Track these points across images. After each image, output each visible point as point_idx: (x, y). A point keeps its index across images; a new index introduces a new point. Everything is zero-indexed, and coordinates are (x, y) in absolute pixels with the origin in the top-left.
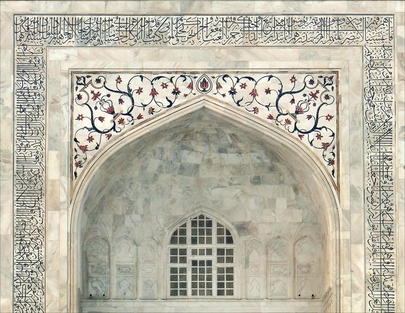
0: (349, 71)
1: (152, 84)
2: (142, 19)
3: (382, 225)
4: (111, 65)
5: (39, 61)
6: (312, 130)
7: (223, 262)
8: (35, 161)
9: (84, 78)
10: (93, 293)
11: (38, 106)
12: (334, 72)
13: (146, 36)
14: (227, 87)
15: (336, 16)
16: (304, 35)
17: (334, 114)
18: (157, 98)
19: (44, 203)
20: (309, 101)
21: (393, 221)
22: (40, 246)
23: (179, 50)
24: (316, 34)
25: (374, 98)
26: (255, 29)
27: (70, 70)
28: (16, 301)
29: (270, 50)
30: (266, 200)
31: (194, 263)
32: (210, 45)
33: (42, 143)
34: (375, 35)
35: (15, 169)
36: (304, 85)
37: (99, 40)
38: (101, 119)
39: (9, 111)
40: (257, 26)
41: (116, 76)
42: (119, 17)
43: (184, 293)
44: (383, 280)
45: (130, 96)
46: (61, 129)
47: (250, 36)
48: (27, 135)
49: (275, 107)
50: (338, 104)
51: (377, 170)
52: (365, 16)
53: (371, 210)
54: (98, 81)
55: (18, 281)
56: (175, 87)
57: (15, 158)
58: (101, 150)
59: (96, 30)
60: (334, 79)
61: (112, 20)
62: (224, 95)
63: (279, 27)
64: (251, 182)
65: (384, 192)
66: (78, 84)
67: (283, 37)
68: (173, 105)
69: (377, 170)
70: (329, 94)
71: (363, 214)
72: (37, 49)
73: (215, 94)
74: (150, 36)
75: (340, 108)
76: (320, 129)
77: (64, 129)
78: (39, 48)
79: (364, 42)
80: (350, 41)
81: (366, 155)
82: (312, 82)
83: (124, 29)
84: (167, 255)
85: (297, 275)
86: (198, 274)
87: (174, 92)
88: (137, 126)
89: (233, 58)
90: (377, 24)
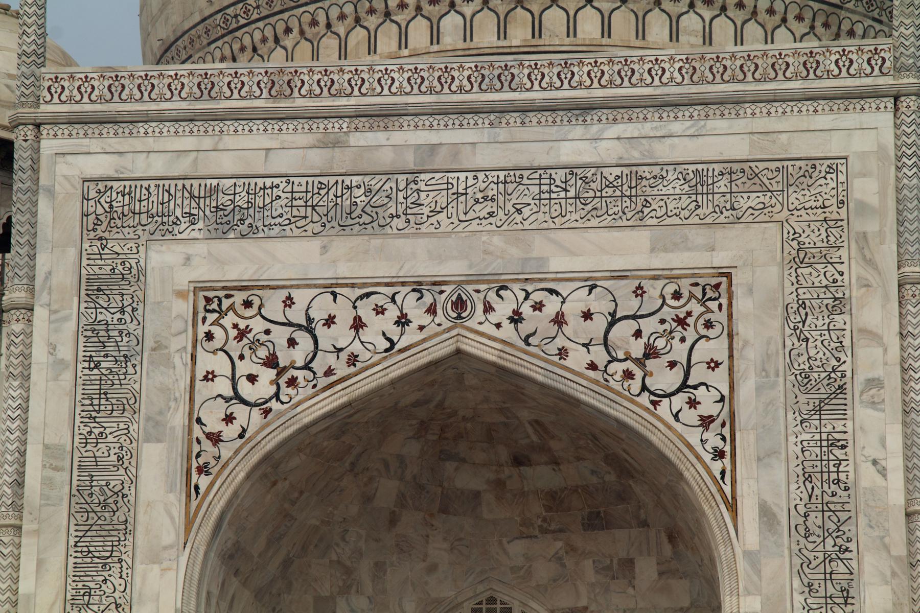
1: (355, 307)
2: (337, 182)
3: (829, 582)
4: (276, 272)
5: (130, 269)
8: (114, 466)
9: (220, 300)
11: (125, 356)
13: (344, 215)
14: (503, 310)
15: (726, 165)
16: (662, 203)
17: (722, 356)
18: (365, 334)
19: (130, 548)
20: (671, 332)
21: (851, 573)
24: (685, 201)
25: (807, 323)
26: (563, 194)
27: (192, 285)
29: (591, 235)
30: (615, 561)
32: (469, 229)
33: (131, 429)
34: (807, 198)
35: (75, 483)
36: (661, 301)
37: (250, 226)
38: (252, 378)
39: (67, 367)
40: (566, 190)
41: (284, 294)
42: (292, 179)
45: (311, 331)
46: (169, 400)
47: (553, 210)
49: (602, 348)
50: (731, 336)
51: (816, 470)
52: (785, 163)
53: (805, 552)
54: (248, 304)
56: (401, 312)
57: (76, 459)
59: (245, 206)
60: (724, 287)
61: (277, 186)
62: (498, 326)
64: (583, 524)
65: (831, 513)
67: (620, 208)
68: (397, 347)
69: (816, 470)
71: (787, 559)
72: (128, 246)
73: (480, 323)
74: (353, 216)
75: (735, 346)
76: (695, 387)
77: (176, 399)
78: (131, 244)
79: (786, 213)
80: (757, 213)
81: (792, 439)
82: (677, 295)
83: (301, 203)
87: (398, 323)
88: (325, 389)
89: (515, 252)
90: (811, 177)
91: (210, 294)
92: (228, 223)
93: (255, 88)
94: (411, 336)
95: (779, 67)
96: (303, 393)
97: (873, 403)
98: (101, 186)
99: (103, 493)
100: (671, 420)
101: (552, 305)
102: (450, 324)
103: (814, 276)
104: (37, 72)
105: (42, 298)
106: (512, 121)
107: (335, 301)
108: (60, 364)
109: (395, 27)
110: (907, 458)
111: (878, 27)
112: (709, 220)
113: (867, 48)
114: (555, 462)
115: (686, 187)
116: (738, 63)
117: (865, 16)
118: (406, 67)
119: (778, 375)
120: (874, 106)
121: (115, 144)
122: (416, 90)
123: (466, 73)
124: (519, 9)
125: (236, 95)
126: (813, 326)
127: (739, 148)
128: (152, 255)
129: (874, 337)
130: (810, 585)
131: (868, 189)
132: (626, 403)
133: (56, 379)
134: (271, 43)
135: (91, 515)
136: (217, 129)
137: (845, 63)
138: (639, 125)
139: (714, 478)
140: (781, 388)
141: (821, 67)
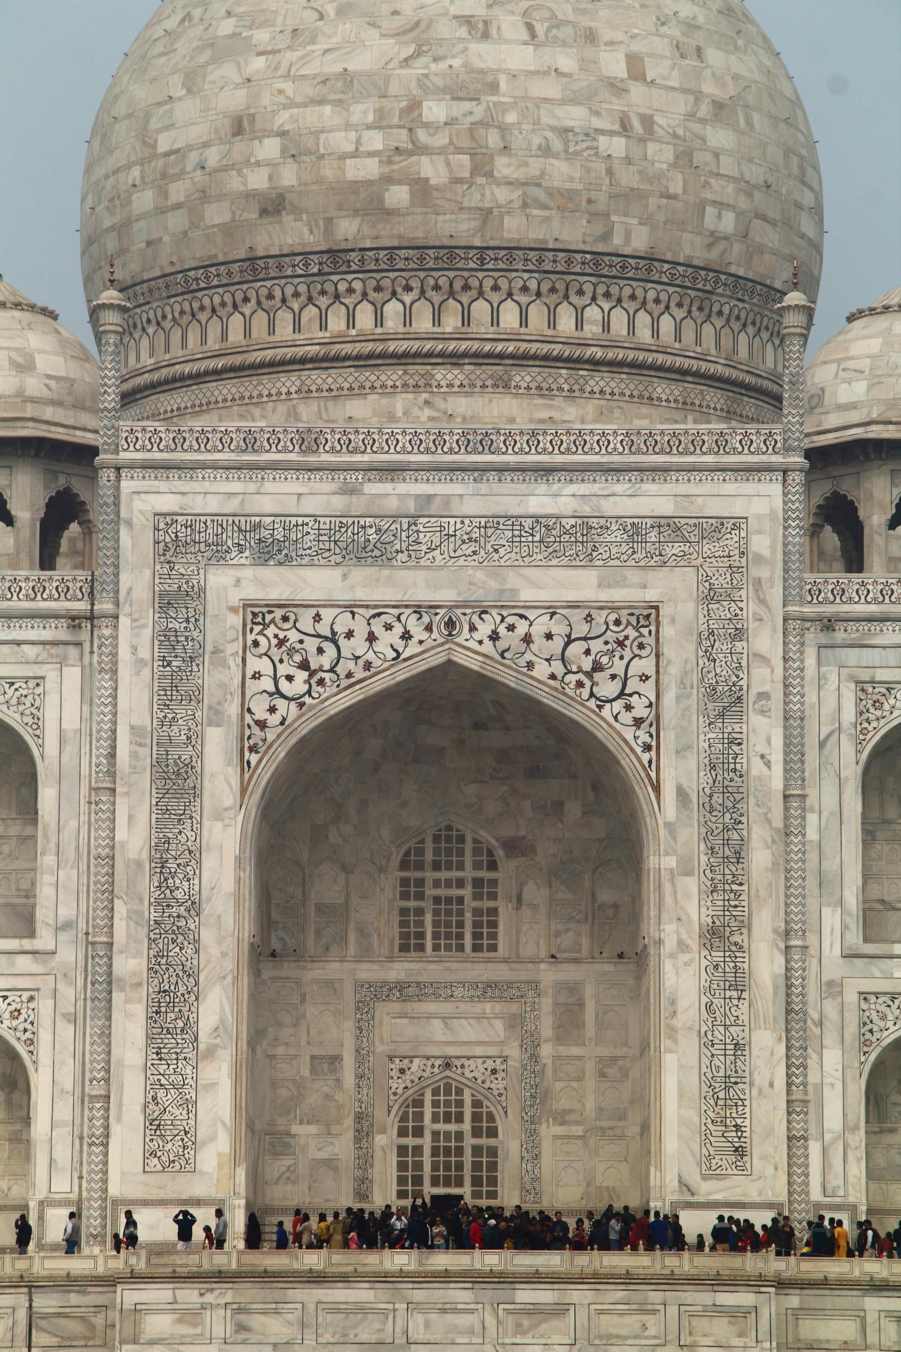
1: (369, 624)
3: (726, 847)
9: (264, 615)
11: (191, 657)
14: (484, 630)
17: (651, 671)
18: (378, 646)
23: (411, 572)
26: (530, 539)
29: (553, 572)
31: (437, 900)
32: (458, 564)
35: (155, 756)
38: (290, 678)
39: (146, 665)
41: (313, 611)
43: (421, 948)
44: (727, 934)
49: (560, 662)
50: (658, 656)
52: (701, 520)
54: (285, 619)
55: (157, 931)
57: (155, 738)
58: (289, 726)
60: (653, 617)
61: (307, 524)
62: (480, 642)
63: (567, 537)
66: (254, 623)
68: (402, 657)
76: (630, 695)
78: (193, 567)
79: (700, 560)
81: (702, 737)
82: (617, 622)
83: (326, 538)
84: (395, 887)
87: (402, 637)
89: (493, 584)
91: (256, 610)
92: (268, 553)
93: (289, 443)
94: (413, 649)
95: (696, 444)
98: (168, 519)
101: (522, 628)
103: (722, 610)
104: (116, 424)
105: (125, 609)
106: (491, 478)
108: (140, 662)
109: (343, 308)
110: (786, 754)
111: (741, 305)
112: (642, 563)
113: (763, 432)
114: (507, 728)
115: (625, 536)
116: (666, 438)
117: (731, 298)
118: (408, 431)
119: (692, 688)
120: (768, 478)
121: (179, 486)
122: (416, 450)
123: (455, 438)
124: (451, 300)
125: (274, 449)
127: (666, 507)
128: (210, 576)
129: (763, 659)
130: (712, 849)
131: (764, 543)
132: (578, 707)
133: (138, 673)
134: (229, 308)
136: (260, 476)
137: (747, 443)
138: (590, 485)
139: (643, 766)
140: (695, 698)
141: (729, 445)
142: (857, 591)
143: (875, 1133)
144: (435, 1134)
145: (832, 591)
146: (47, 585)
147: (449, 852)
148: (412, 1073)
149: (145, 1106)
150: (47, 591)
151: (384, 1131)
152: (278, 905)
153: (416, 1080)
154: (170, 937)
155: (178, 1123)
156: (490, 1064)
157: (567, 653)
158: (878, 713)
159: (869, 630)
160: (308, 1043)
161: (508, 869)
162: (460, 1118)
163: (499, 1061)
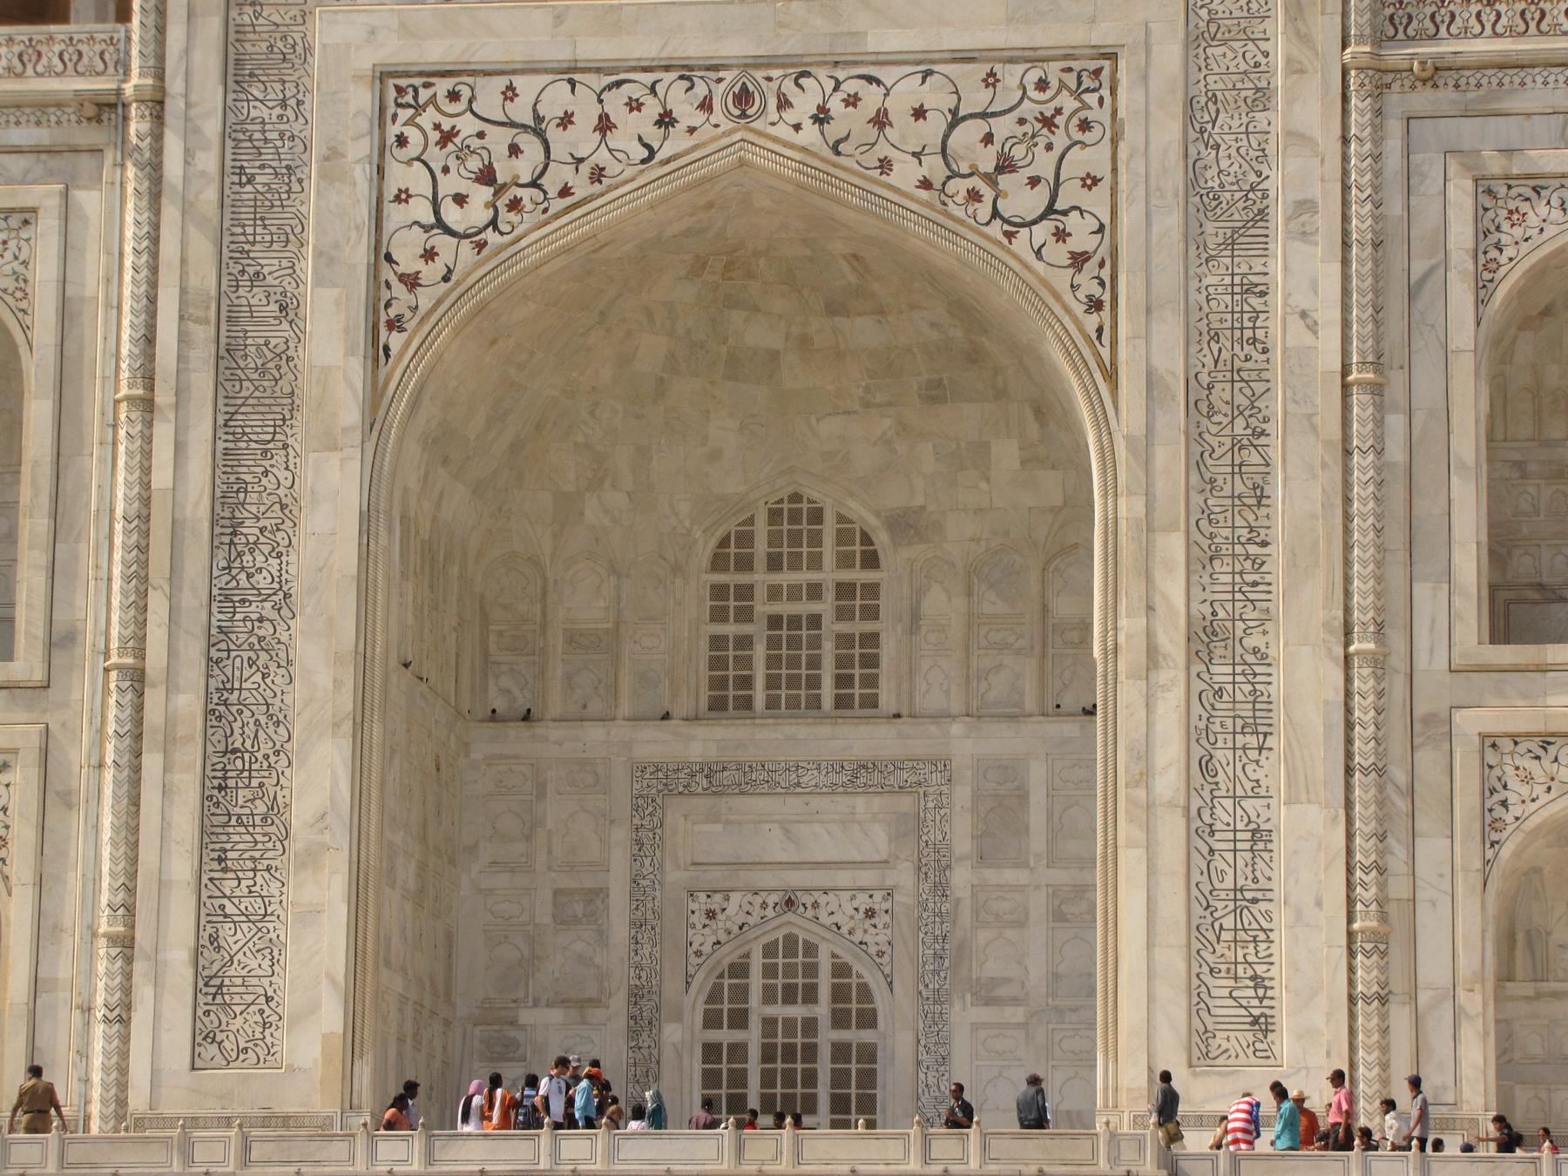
0: (1148, 52)
1: (601, 101)
4: (489, 52)
5: (293, 47)
6: (1042, 217)
7: (853, 619)
10: (500, 704)
11: (288, 168)
12: (1105, 56)
14: (805, 104)
17: (1104, 170)
18: (614, 139)
20: (1033, 136)
21: (1268, 465)
22: (284, 550)
27: (379, 69)
28: (215, 700)
30: (963, 445)
31: (774, 622)
35: (223, 341)
38: (460, 200)
41: (503, 81)
43: (746, 704)
44: (1239, 633)
45: (540, 134)
48: (258, 247)
49: (939, 157)
50: (1114, 142)
51: (1226, 325)
53: (1206, 436)
54: (454, 96)
55: (223, 646)
57: (224, 308)
58: (458, 283)
60: (1106, 73)
62: (797, 127)
66: (399, 105)
68: (658, 157)
69: (1226, 325)
70: (1090, 115)
72: (291, 14)
73: (773, 124)
76: (1065, 213)
78: (294, 11)
81: (1194, 284)
82: (1042, 85)
85: (1050, 651)
86: (784, 651)
88: (557, 216)
91: (403, 82)
94: (676, 142)
96: (529, 219)
97: (1304, 233)
99: (261, 355)
100: (1030, 258)
102: (732, 125)
107: (573, 91)
126: (1226, 128)
132: (970, 235)
135: (246, 384)
139: (1087, 338)
142: (1478, 15)
143: (1527, 998)
144: (769, 1023)
145: (1433, 16)
146: (43, 49)
147: (795, 538)
148: (728, 918)
149: (197, 953)
150: (44, 61)
151: (678, 1017)
152: (500, 634)
153: (736, 929)
154: (245, 655)
155: (255, 981)
156: (863, 901)
157: (950, 142)
158: (1518, 232)
159: (1500, 84)
160: (549, 868)
161: (895, 560)
162: (811, 995)
163: (878, 896)
